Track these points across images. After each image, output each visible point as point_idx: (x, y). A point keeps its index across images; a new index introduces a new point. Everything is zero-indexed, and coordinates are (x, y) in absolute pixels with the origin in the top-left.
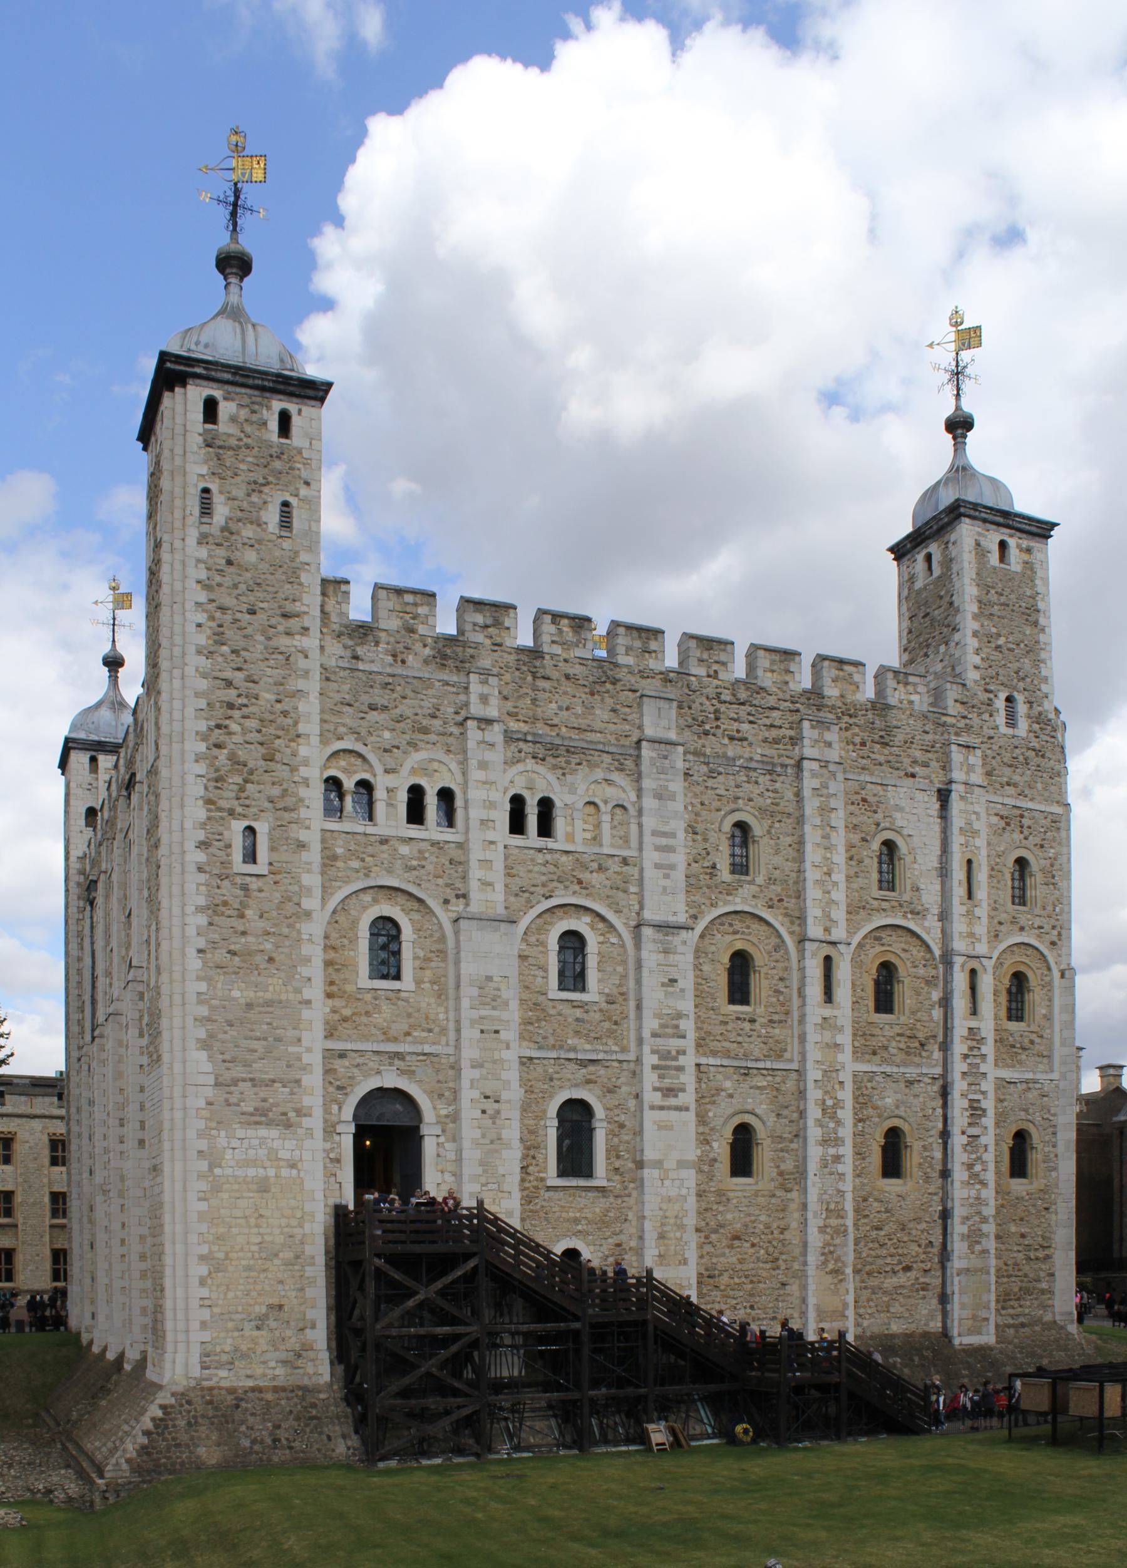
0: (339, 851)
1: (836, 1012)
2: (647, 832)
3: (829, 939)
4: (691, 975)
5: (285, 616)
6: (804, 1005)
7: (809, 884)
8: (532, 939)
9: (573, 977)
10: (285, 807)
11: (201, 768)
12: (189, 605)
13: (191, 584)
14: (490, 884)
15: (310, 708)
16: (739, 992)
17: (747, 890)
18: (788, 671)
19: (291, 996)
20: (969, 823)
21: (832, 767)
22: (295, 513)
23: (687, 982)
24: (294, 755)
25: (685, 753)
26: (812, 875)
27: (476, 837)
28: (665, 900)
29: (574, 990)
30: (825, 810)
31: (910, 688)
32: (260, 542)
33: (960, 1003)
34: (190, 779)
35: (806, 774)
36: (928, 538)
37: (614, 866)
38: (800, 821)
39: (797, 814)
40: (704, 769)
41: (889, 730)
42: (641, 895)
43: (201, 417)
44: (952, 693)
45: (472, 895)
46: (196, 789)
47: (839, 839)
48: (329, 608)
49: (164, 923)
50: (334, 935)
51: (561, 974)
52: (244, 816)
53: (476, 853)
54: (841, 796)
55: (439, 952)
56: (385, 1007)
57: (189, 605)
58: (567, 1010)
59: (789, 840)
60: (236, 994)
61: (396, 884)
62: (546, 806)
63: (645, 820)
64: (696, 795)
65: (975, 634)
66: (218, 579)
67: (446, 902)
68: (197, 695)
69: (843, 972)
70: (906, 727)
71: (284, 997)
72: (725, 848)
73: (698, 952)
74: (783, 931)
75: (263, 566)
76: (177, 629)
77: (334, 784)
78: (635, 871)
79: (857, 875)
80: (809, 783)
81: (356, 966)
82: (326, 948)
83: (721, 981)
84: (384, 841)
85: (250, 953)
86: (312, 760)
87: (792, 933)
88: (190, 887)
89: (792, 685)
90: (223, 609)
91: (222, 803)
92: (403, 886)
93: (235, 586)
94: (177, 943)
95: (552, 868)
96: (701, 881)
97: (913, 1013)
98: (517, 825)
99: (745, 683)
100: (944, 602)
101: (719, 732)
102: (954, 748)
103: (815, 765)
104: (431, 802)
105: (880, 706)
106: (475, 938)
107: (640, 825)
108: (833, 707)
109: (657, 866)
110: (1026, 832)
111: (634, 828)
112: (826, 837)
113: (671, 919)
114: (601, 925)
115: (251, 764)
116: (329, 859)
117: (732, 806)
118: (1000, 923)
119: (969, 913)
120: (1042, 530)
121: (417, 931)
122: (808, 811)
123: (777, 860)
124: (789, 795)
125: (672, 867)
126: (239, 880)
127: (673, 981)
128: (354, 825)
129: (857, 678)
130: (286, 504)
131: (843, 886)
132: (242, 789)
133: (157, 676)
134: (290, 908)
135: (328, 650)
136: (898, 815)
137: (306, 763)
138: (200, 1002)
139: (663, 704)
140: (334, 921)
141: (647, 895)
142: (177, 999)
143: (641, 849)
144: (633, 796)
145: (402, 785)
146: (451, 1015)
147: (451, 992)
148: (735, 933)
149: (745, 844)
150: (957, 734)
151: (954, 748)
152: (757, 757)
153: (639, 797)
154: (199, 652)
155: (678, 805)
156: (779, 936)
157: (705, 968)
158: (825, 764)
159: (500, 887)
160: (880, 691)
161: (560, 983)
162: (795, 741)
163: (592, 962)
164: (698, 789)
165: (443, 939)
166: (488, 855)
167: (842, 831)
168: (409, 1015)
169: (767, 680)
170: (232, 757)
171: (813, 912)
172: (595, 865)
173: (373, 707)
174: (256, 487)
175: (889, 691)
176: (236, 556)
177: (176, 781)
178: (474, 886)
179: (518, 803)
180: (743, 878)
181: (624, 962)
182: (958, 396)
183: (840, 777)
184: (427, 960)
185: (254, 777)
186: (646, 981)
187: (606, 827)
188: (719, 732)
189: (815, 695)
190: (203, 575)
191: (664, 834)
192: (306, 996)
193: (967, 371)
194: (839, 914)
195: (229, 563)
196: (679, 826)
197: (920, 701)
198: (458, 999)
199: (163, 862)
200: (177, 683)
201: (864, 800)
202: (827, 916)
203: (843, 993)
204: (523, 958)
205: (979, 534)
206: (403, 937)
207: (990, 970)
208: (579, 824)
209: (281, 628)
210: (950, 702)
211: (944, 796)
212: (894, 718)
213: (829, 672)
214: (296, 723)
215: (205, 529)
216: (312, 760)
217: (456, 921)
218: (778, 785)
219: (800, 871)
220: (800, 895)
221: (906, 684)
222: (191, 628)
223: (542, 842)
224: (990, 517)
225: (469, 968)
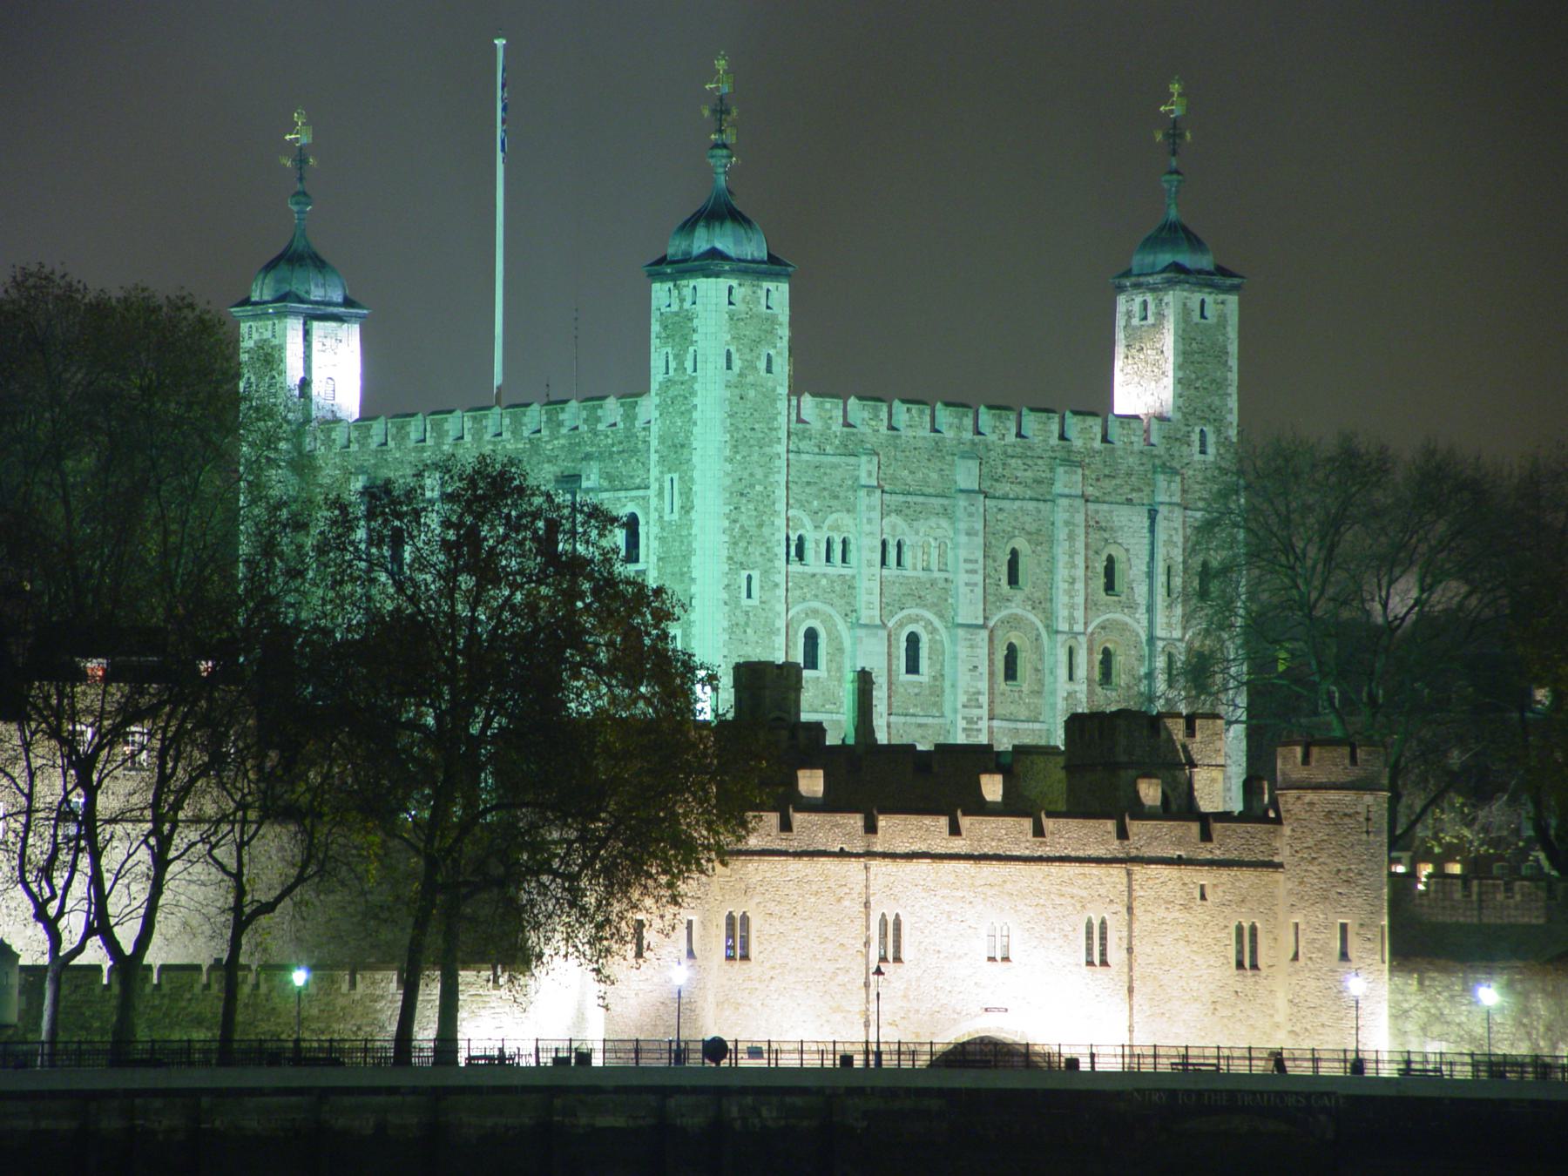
16: (1011, 673)
28: (969, 609)
77: (788, 539)
84: (814, 575)
107: (956, 556)
125: (976, 585)
128: (795, 567)
143: (956, 572)
145: (822, 536)
171: (1063, 613)
173: (808, 483)
191: (970, 561)
194: (1079, 614)
196: (979, 555)
211: (1153, 515)
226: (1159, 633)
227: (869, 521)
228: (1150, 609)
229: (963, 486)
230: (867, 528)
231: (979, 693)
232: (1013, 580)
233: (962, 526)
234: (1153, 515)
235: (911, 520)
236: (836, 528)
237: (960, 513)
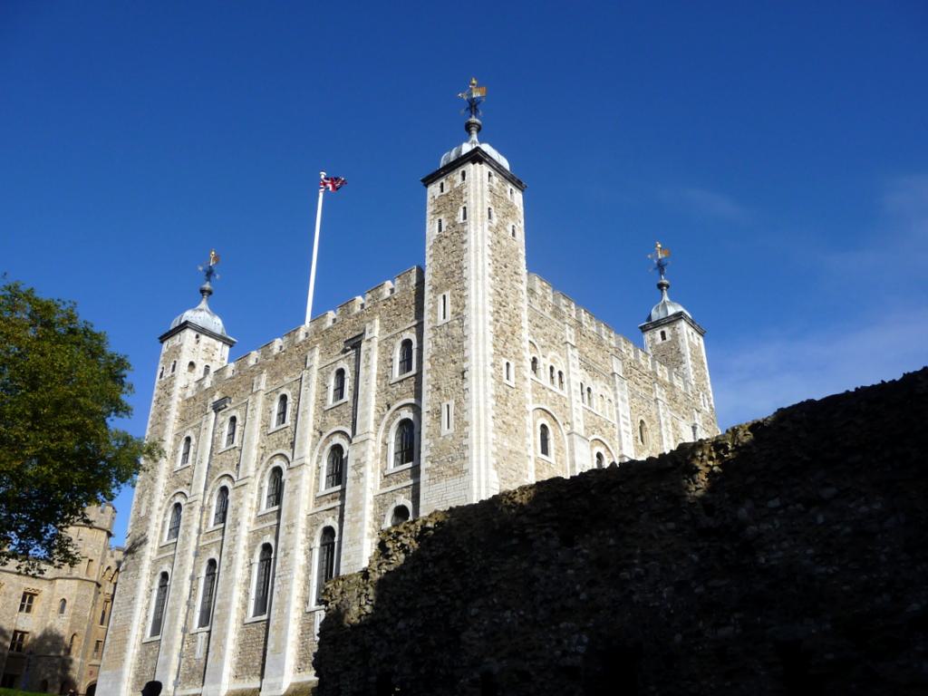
5: (515, 273)
15: (525, 315)
46: (490, 338)
61: (548, 409)
75: (508, 248)
88: (489, 384)
100: (674, 352)
132: (505, 344)
190: (490, 244)
227: (574, 365)
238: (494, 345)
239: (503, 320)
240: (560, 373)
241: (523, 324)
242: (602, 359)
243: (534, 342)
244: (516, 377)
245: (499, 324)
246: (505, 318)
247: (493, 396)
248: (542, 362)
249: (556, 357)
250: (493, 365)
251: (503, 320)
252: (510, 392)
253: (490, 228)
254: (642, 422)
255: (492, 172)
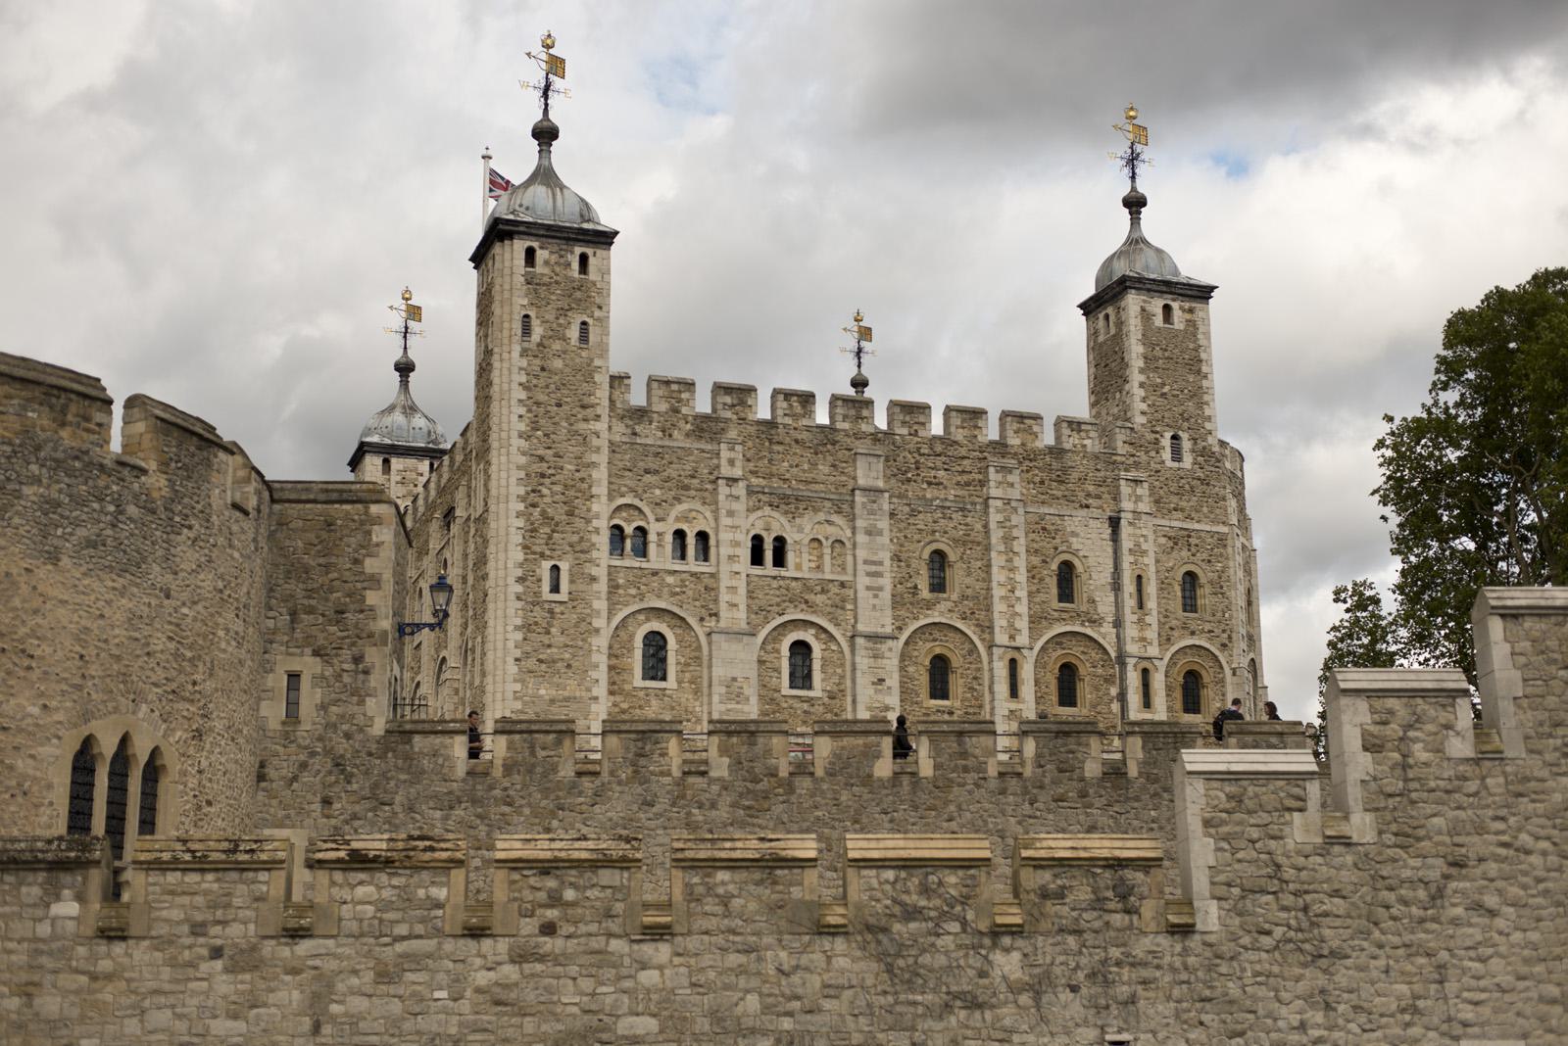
0: (621, 581)
1: (1021, 706)
2: (860, 561)
3: (1013, 644)
4: (896, 676)
5: (584, 407)
6: (993, 700)
7: (996, 600)
8: (769, 647)
9: (801, 677)
10: (581, 550)
11: (521, 523)
12: (514, 402)
13: (515, 386)
14: (735, 605)
15: (601, 475)
17: (943, 606)
18: (976, 427)
19: (584, 694)
20: (1138, 545)
21: (1014, 504)
22: (591, 329)
23: (893, 681)
24: (589, 510)
25: (890, 497)
26: (998, 592)
27: (725, 569)
28: (874, 614)
29: (802, 688)
30: (1008, 539)
31: (1083, 434)
32: (564, 352)
33: (1134, 698)
34: (513, 530)
35: (991, 510)
36: (1106, 302)
37: (835, 589)
38: (988, 548)
39: (985, 542)
40: (907, 509)
41: (1065, 470)
42: (855, 611)
43: (523, 262)
44: (1120, 437)
45: (722, 614)
47: (1021, 562)
48: (615, 397)
49: (490, 638)
50: (616, 646)
51: (792, 675)
52: (552, 558)
53: (725, 581)
54: (1022, 527)
55: (695, 658)
56: (654, 702)
57: (514, 402)
58: (797, 705)
59: (979, 564)
60: (542, 692)
62: (780, 544)
63: (858, 552)
64: (900, 531)
65: (1142, 385)
66: (535, 381)
67: (702, 619)
68: (519, 468)
69: (1027, 672)
70: (1080, 466)
71: (578, 694)
72: (924, 572)
73: (903, 657)
74: (975, 639)
76: (505, 419)
78: (851, 592)
79: (1038, 591)
80: (994, 518)
81: (631, 671)
82: (610, 656)
83: (923, 680)
84: (655, 573)
85: (554, 662)
86: (601, 512)
87: (983, 640)
88: (511, 612)
89: (980, 438)
90: (538, 404)
91: (537, 549)
92: (669, 608)
93: (547, 387)
94: (500, 654)
95: (784, 592)
96: (904, 600)
97: (1094, 706)
98: (757, 558)
99: (940, 438)
101: (919, 479)
102: (1122, 482)
103: (999, 503)
104: (691, 541)
105: (1057, 452)
106: (724, 648)
107: (854, 556)
108: (1016, 454)
109: (868, 588)
110: (1193, 549)
111: (850, 558)
112: (1010, 560)
113: (880, 630)
114: (823, 636)
115: (557, 518)
116: (613, 587)
117: (930, 538)
118: (1172, 629)
119: (1140, 621)
120: (1204, 293)
121: (679, 642)
122: (994, 540)
123: (968, 581)
124: (978, 527)
125: (880, 589)
126: (546, 606)
127: (881, 680)
129: (1036, 428)
130: (584, 323)
131: (1025, 601)
132: (550, 538)
133: (488, 450)
134: (583, 626)
135: (614, 429)
136: (1074, 540)
137: (597, 516)
138: (516, 699)
139: (871, 459)
140: (615, 635)
141: (860, 611)
142: (499, 696)
144: (849, 533)
145: (669, 528)
146: (705, 707)
147: (705, 690)
148: (935, 640)
149: (942, 568)
150: (1126, 470)
151: (1122, 482)
152: (951, 498)
153: (854, 533)
154: (520, 437)
155: (885, 539)
156: (972, 642)
157: (911, 669)
158: (1008, 502)
159: (743, 607)
160: (1058, 438)
161: (791, 681)
162: (983, 483)
163: (816, 665)
164: (902, 525)
165: (699, 648)
166: (734, 583)
167: (1023, 555)
168: (673, 708)
169: (959, 435)
170: (543, 513)
171: (1000, 622)
172: (819, 588)
174: (563, 312)
175: (1064, 438)
176: (548, 364)
177: (502, 532)
178: (723, 606)
179: (757, 542)
180: (941, 595)
181: (842, 665)
182: (1133, 178)
183: (1021, 511)
184: (687, 665)
185: (560, 528)
186: (859, 680)
187: (827, 559)
188: (919, 479)
189: (1000, 447)
190: (524, 379)
191: (874, 563)
192: (595, 692)
193: (1142, 157)
194: (1023, 624)
195: (543, 369)
196: (886, 556)
197: (1092, 444)
198: (710, 695)
199: (491, 592)
200: (503, 459)
201: (1044, 529)
202: (1011, 625)
203: (1027, 690)
204: (761, 662)
205: (1144, 301)
206: (669, 647)
207: (1162, 670)
208: (806, 556)
209: (580, 416)
210: (1120, 444)
211: (1115, 523)
212: (1069, 460)
213: (1012, 426)
214: (590, 487)
215: (526, 345)
216: (601, 512)
217: (709, 634)
218: (969, 520)
219: (989, 589)
220: (989, 609)
221: (1080, 431)
222: (514, 418)
223: (776, 571)
224: (1155, 287)
225: (719, 672)
226: (1132, 648)
227: (731, 514)
228: (1118, 624)
229: (861, 482)
230: (728, 521)
231: (887, 708)
232: (938, 586)
233: (860, 523)
234: (1115, 523)
235: (793, 516)
236: (686, 519)
237: (858, 510)
238: (525, 547)
239: (548, 500)
240: (702, 536)
241: (594, 491)
242: (826, 469)
243: (637, 502)
244: (572, 582)
245: (536, 512)
246: (553, 494)
247: (517, 628)
248: (653, 528)
249: (691, 510)
250: (521, 580)
251: (546, 500)
252: (558, 609)
253: (524, 353)
254: (939, 559)
255: (535, 245)
